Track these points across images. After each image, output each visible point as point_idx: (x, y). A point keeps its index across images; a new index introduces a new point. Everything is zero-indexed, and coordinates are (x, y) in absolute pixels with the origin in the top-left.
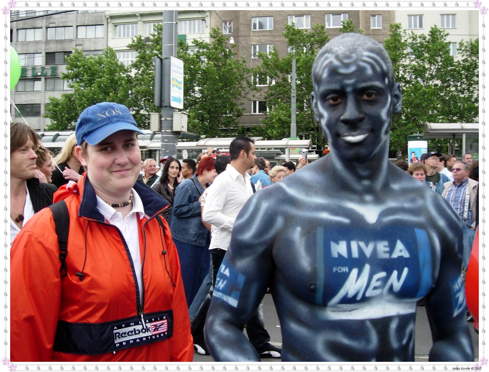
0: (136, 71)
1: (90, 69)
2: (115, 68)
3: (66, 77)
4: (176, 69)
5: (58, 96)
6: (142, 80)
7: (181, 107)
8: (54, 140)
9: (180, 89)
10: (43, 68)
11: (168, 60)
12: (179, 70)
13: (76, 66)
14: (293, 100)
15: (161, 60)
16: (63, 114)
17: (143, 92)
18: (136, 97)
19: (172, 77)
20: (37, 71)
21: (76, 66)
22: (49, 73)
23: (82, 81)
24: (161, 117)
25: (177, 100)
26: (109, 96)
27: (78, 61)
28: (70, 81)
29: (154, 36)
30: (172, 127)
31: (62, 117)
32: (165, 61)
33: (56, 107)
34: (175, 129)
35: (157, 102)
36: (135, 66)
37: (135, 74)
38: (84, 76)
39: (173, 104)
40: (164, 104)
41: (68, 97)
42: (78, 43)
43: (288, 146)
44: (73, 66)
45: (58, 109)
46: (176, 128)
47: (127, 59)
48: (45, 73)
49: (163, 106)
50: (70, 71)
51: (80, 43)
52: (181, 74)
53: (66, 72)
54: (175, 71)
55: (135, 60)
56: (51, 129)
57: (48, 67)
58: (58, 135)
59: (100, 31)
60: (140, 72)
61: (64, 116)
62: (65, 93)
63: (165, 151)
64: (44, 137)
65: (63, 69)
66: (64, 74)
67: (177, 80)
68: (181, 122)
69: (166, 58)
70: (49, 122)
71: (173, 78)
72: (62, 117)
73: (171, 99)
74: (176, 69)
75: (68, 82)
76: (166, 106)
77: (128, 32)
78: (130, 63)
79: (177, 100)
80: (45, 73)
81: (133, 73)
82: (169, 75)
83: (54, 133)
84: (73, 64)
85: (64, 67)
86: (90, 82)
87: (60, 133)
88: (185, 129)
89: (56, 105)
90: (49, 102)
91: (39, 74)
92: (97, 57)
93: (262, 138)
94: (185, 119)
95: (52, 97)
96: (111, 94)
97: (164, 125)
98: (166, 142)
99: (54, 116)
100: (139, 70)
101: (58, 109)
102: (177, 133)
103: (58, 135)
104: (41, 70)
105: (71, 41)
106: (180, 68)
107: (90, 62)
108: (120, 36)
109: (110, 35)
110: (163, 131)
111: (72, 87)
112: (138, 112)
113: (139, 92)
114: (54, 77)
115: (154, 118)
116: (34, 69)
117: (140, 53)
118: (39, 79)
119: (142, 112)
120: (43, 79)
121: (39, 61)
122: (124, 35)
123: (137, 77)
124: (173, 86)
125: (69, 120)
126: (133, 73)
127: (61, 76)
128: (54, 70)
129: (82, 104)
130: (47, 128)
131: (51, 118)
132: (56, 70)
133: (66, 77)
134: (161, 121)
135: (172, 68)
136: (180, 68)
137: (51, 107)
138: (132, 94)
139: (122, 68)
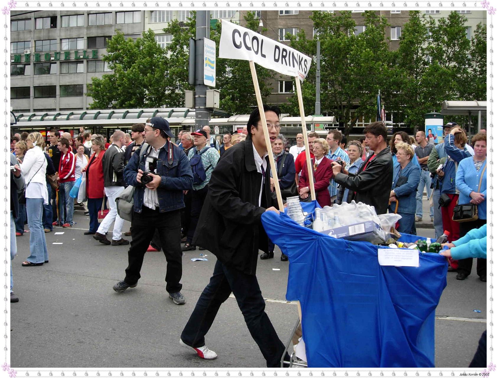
0: (172, 53)
1: (129, 51)
2: (153, 50)
3: (107, 59)
4: (208, 49)
5: (100, 77)
7: (213, 85)
8: (96, 118)
9: (213, 68)
10: (85, 52)
12: (212, 51)
13: (116, 49)
14: (318, 80)
15: (195, 41)
16: (104, 94)
18: (171, 77)
19: (205, 57)
21: (116, 49)
22: (91, 56)
23: (121, 62)
24: (194, 94)
26: (147, 76)
27: (119, 44)
28: (111, 62)
30: (205, 104)
31: (103, 97)
32: (198, 43)
33: (98, 87)
34: (207, 106)
36: (171, 48)
37: (171, 56)
38: (123, 58)
39: (207, 82)
40: (198, 82)
41: (110, 77)
43: (313, 122)
44: (114, 49)
46: (209, 105)
47: (164, 42)
48: (87, 56)
49: (197, 85)
52: (213, 54)
54: (208, 52)
56: (93, 109)
57: (90, 50)
58: (99, 113)
60: (175, 54)
61: (105, 95)
62: (105, 74)
64: (87, 115)
65: (103, 52)
66: (104, 56)
67: (209, 60)
68: (213, 99)
70: (91, 101)
71: (206, 58)
73: (205, 77)
74: (208, 49)
75: (109, 63)
76: (200, 85)
78: (165, 46)
80: (87, 56)
83: (96, 111)
84: (114, 47)
86: (129, 65)
87: (101, 111)
88: (217, 106)
89: (97, 84)
91: (82, 57)
92: (135, 41)
93: (288, 114)
94: (217, 96)
96: (148, 74)
97: (198, 102)
98: (200, 118)
99: (96, 96)
100: (175, 52)
101: (100, 89)
102: (210, 110)
103: (99, 113)
104: (83, 54)
106: (212, 48)
107: (130, 45)
110: (196, 107)
111: (112, 69)
113: (174, 73)
114: (96, 59)
115: (189, 95)
116: (77, 52)
117: (175, 36)
118: (82, 62)
119: (177, 91)
120: (85, 61)
121: (82, 45)
123: (173, 59)
124: (206, 66)
125: (110, 99)
126: (169, 54)
127: (102, 58)
128: (95, 53)
129: (122, 84)
130: (89, 107)
131: (93, 97)
133: (107, 59)
134: (195, 99)
136: (212, 48)
137: (94, 87)
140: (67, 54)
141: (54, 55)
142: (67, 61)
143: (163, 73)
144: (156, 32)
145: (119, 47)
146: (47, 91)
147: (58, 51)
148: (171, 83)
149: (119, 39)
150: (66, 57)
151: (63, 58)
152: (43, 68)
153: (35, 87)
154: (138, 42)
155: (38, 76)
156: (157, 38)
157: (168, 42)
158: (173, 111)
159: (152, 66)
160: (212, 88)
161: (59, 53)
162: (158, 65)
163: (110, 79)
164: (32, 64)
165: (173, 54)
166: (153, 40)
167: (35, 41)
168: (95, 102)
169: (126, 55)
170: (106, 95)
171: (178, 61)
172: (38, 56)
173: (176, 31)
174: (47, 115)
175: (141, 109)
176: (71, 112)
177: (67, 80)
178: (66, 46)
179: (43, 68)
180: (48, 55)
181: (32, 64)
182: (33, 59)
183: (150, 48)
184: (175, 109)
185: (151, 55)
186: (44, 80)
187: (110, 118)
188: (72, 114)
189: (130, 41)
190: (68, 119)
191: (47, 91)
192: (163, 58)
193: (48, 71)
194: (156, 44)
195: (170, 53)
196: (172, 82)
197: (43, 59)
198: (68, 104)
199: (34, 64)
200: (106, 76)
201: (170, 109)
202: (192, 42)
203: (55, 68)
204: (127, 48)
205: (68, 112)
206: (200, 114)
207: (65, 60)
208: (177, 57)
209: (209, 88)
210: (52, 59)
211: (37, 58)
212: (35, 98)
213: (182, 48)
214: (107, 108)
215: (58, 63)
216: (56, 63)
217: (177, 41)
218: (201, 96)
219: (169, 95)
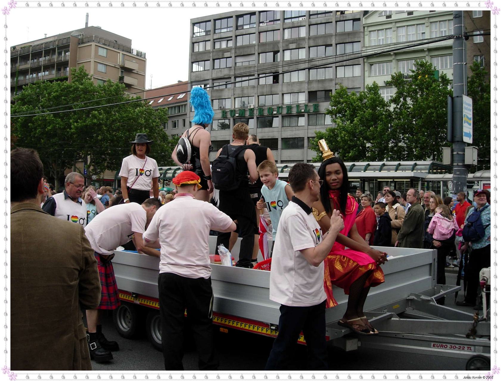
0: (395, 106)
1: (352, 105)
3: (330, 112)
4: (466, 106)
6: (401, 114)
10: (306, 106)
11: (459, 98)
13: (339, 103)
15: (452, 98)
17: (401, 125)
18: (394, 131)
20: (301, 108)
21: (339, 103)
22: (312, 110)
23: (344, 116)
24: (452, 151)
25: (468, 135)
28: (334, 116)
29: (413, 72)
30: (464, 161)
32: (457, 100)
34: (467, 162)
35: (449, 138)
36: (395, 101)
37: (395, 109)
38: (346, 111)
40: (457, 139)
41: (332, 130)
42: (337, 81)
44: (336, 103)
46: (468, 161)
47: (387, 95)
48: (308, 109)
49: (456, 140)
50: (333, 107)
53: (330, 108)
54: (466, 109)
55: (394, 96)
57: (311, 104)
59: (357, 71)
60: (399, 107)
62: (329, 127)
63: (457, 183)
65: (325, 106)
66: (328, 110)
67: (467, 117)
69: (458, 97)
74: (466, 106)
75: (332, 117)
76: (458, 141)
77: (383, 70)
79: (468, 135)
81: (392, 107)
82: (462, 112)
85: (329, 103)
90: (314, 135)
91: (303, 111)
92: (358, 95)
95: (318, 131)
97: (456, 158)
98: (458, 175)
104: (304, 108)
105: (331, 80)
107: (352, 99)
108: (375, 74)
109: (367, 74)
110: (454, 164)
112: (396, 145)
114: (317, 112)
116: (298, 106)
117: (398, 89)
118: (303, 116)
119: (400, 144)
120: (306, 115)
121: (303, 99)
123: (396, 112)
126: (392, 107)
127: (326, 112)
128: (316, 107)
132: (318, 107)
133: (330, 112)
134: (452, 155)
135: (464, 105)
138: (392, 126)
139: (383, 104)
140: (289, 107)
141: (277, 110)
142: (289, 115)
143: (386, 125)
144: (380, 85)
145: (342, 100)
147: (280, 105)
148: (394, 136)
149: (342, 93)
150: (288, 111)
151: (285, 112)
152: (266, 121)
154: (361, 96)
155: (260, 130)
156: (381, 92)
157: (391, 95)
158: (399, 165)
159: (375, 118)
160: (469, 145)
161: (282, 107)
162: (382, 118)
164: (255, 117)
165: (397, 107)
166: (376, 93)
167: (258, 96)
169: (349, 108)
171: (401, 114)
173: (399, 84)
175: (368, 163)
177: (289, 133)
178: (288, 100)
179: (266, 121)
180: (270, 109)
181: (255, 117)
182: (256, 113)
183: (374, 101)
184: (402, 163)
185: (374, 108)
189: (353, 94)
192: (386, 111)
193: (270, 125)
194: (379, 96)
195: (393, 106)
196: (395, 135)
197: (266, 113)
199: (257, 118)
201: (396, 163)
202: (449, 99)
203: (276, 122)
204: (350, 102)
206: (458, 170)
208: (400, 109)
209: (466, 145)
210: (275, 112)
211: (260, 112)
213: (405, 99)
215: (280, 116)
216: (278, 117)
217: (400, 94)
218: (459, 153)
219: (392, 148)
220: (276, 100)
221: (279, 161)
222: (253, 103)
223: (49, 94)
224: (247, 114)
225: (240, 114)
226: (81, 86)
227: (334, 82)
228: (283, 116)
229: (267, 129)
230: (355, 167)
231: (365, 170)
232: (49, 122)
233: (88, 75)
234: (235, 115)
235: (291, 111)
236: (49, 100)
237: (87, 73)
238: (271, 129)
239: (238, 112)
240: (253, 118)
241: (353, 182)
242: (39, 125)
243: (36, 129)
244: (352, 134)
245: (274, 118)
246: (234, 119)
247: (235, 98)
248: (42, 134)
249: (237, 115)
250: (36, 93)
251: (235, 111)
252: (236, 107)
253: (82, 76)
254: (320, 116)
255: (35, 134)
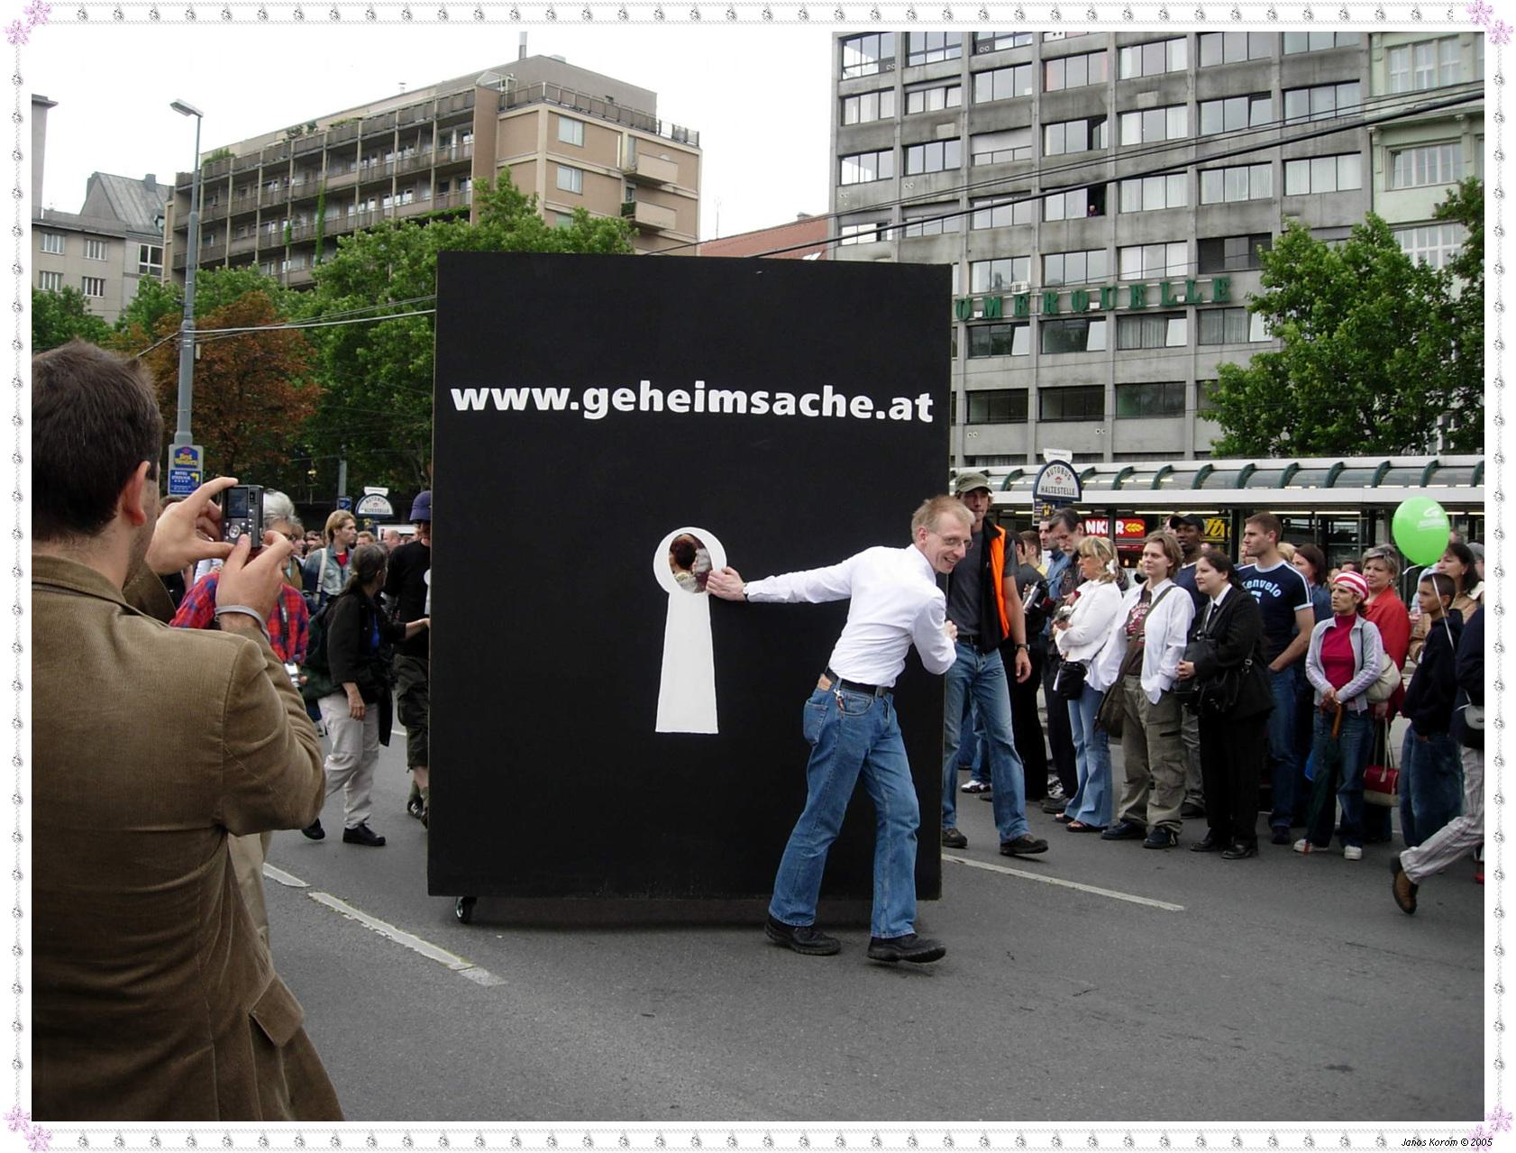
3: (1263, 306)
5: (1244, 363)
8: (1241, 483)
10: (1191, 284)
20: (1175, 291)
21: (1291, 276)
22: (1209, 296)
42: (1287, 207)
45: (1242, 397)
48: (1196, 295)
51: (1295, 207)
53: (1263, 292)
56: (1222, 455)
57: (1206, 279)
59: (1350, 172)
65: (1249, 284)
66: (1255, 299)
70: (1213, 432)
72: (1254, 419)
83: (1241, 464)
87: (1258, 463)
89: (1236, 382)
90: (1216, 375)
91: (1181, 299)
95: (1226, 362)
101: (1242, 397)
103: (1252, 468)
105: (1267, 203)
108: (1408, 182)
109: (1380, 182)
114: (1224, 304)
116: (1166, 285)
118: (1182, 315)
120: (1191, 312)
121: (1180, 261)
122: (1421, 178)
125: (1274, 429)
128: (1223, 287)
130: (1213, 449)
133: (1263, 306)
137: (1223, 391)
140: (1139, 290)
142: (1139, 314)
146: (1078, 403)
147: (1110, 284)
150: (1135, 299)
151: (1125, 303)
152: (1065, 333)
153: (1041, 390)
155: (1047, 359)
161: (1115, 289)
163: (1274, 367)
164: (1034, 322)
167: (1043, 256)
168: (1230, 438)
170: (1260, 415)
172: (1051, 297)
174: (1130, 472)
175: (1384, 459)
176: (1166, 464)
177: (1137, 370)
178: (1134, 266)
179: (1065, 333)
180: (1081, 297)
181: (1034, 322)
182: (1036, 308)
186: (1068, 370)
187: (1286, 481)
188: (1169, 470)
190: (1156, 486)
191: (1078, 403)
193: (1080, 344)
197: (1066, 307)
198: (1140, 442)
200: (1265, 360)
203: (1099, 334)
205: (1158, 465)
207: (1131, 308)
210: (1094, 306)
211: (1047, 306)
212: (1041, 421)
214: (1262, 452)
215: (1111, 317)
216: (1103, 318)
220: (1097, 267)
221: (1108, 455)
222: (1025, 277)
223: (416, 261)
224: (1010, 312)
225: (986, 313)
226: (509, 235)
227: (1277, 209)
228: (1118, 318)
229: (1070, 357)
230: (1344, 472)
231: (1377, 482)
232: (417, 345)
233: (525, 200)
234: (971, 315)
235: (1144, 301)
236: (415, 277)
237: (522, 193)
238: (1081, 356)
239: (982, 306)
240: (1027, 324)
241: (1338, 518)
242: (388, 354)
243: (377, 364)
244: (1336, 372)
245: (1092, 324)
246: (968, 328)
247: (971, 264)
248: (398, 377)
249: (978, 314)
250: (378, 258)
251: (971, 301)
252: (976, 290)
253: (508, 202)
254: (1234, 315)
255: (376, 378)
